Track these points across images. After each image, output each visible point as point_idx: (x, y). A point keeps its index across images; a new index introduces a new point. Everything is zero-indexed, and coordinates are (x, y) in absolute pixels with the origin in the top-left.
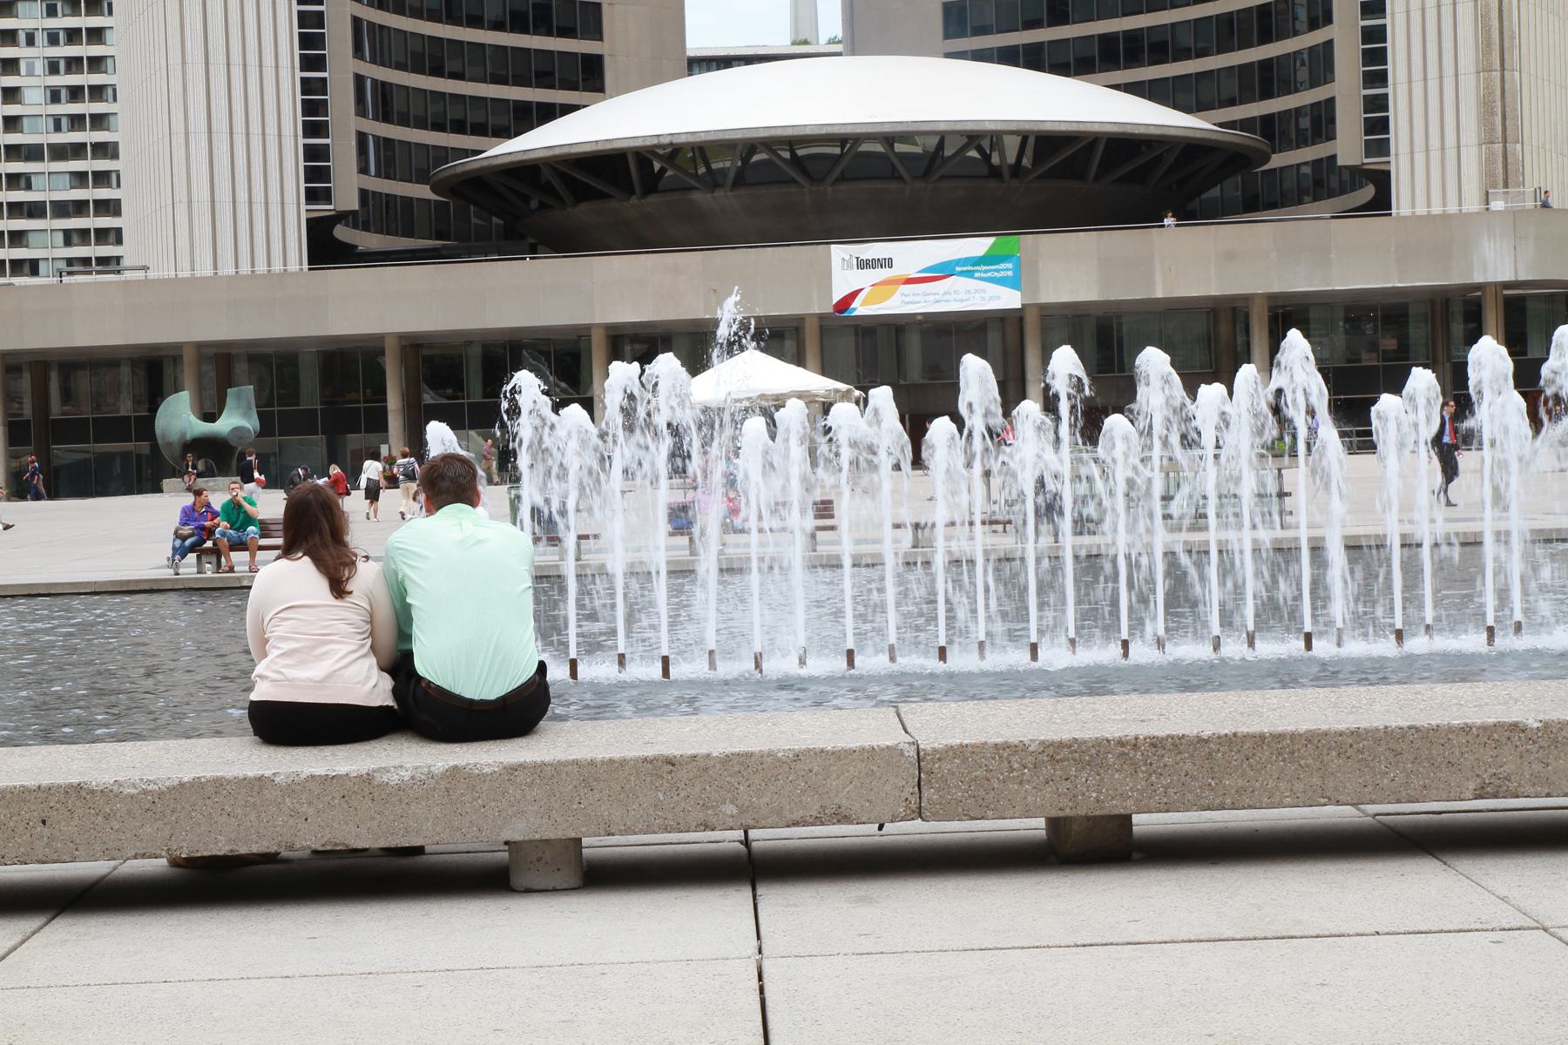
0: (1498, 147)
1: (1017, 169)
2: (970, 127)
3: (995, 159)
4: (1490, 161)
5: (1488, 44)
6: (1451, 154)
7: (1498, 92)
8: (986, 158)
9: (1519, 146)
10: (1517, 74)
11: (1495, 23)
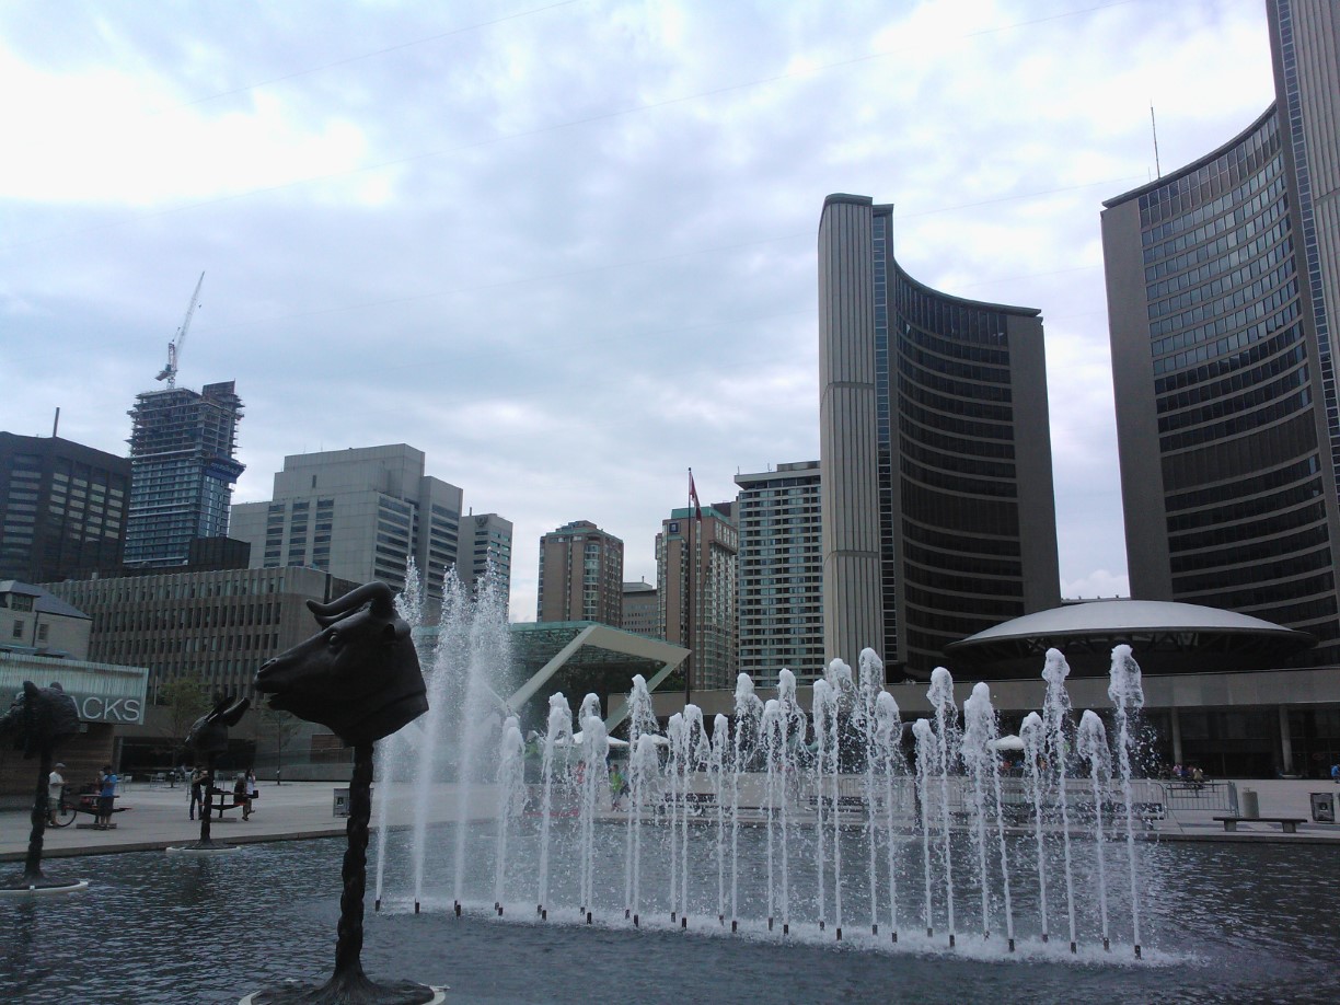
1: (1191, 647)
3: (1179, 643)
8: (1176, 642)
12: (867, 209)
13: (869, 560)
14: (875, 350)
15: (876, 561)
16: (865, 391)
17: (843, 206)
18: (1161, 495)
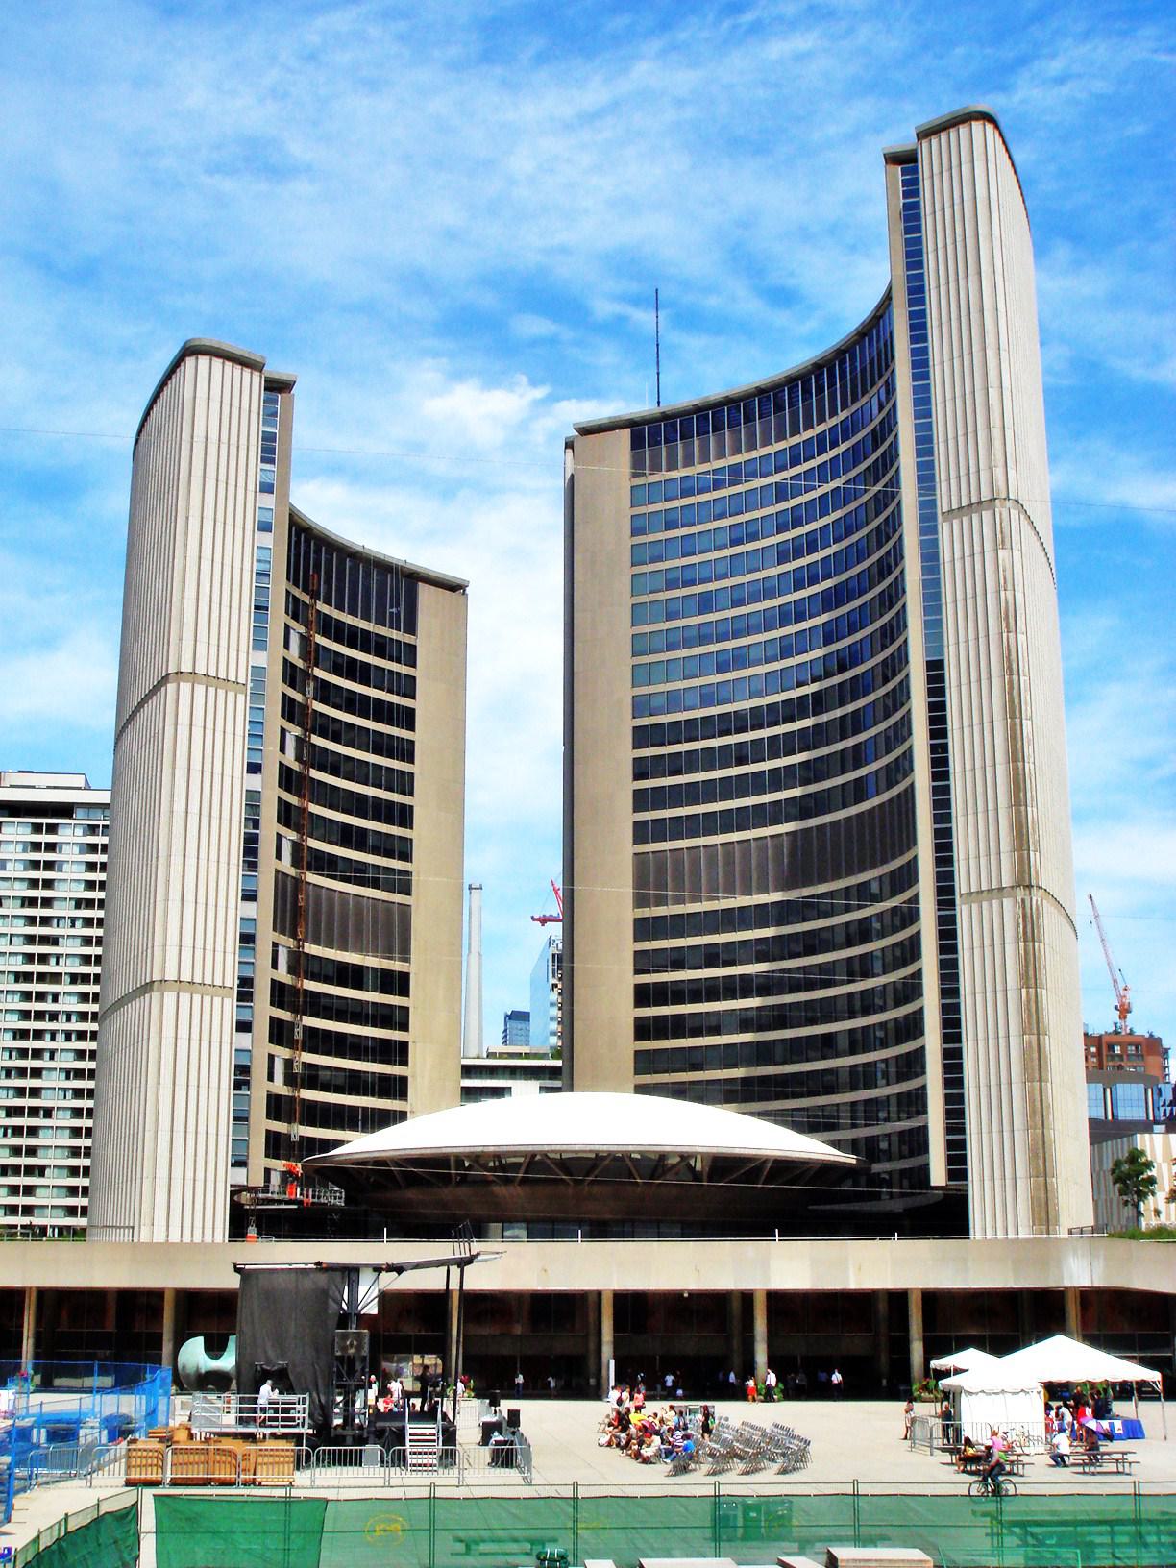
0: (1042, 1179)
2: (679, 1149)
4: (1037, 1188)
5: (1034, 1112)
6: (1008, 1182)
7: (1041, 1143)
9: (1054, 1180)
10: (1052, 1131)
11: (1038, 1098)
12: (256, 375)
13: (217, 1001)
14: (252, 624)
15: (228, 1002)
16: (231, 695)
17: (217, 363)
18: (628, 914)
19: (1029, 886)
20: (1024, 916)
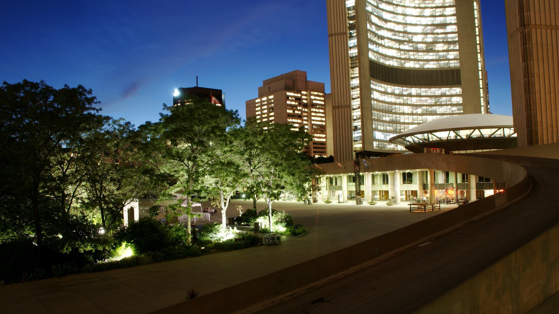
19: (525, 25)
20: (523, 37)
